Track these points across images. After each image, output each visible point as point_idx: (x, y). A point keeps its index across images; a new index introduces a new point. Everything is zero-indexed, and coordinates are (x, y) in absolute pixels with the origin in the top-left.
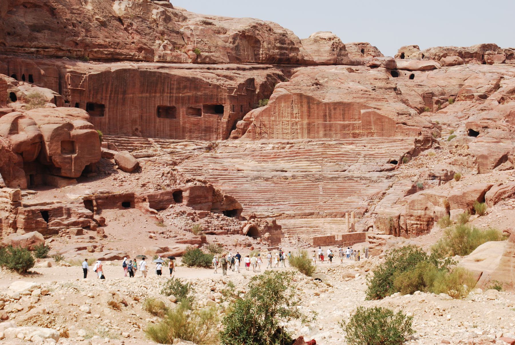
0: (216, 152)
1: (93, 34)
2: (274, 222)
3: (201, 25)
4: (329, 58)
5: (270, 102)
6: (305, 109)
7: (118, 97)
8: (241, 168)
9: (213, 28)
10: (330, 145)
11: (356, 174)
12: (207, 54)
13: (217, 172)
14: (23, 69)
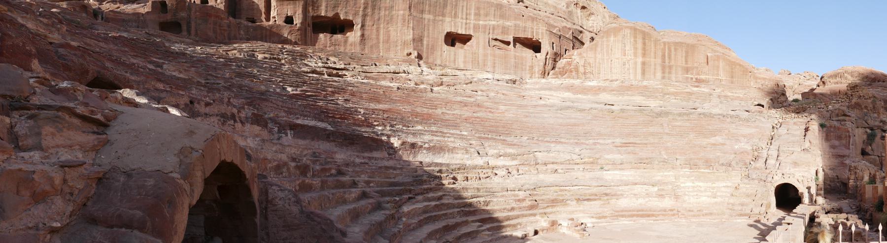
6: (640, 45)
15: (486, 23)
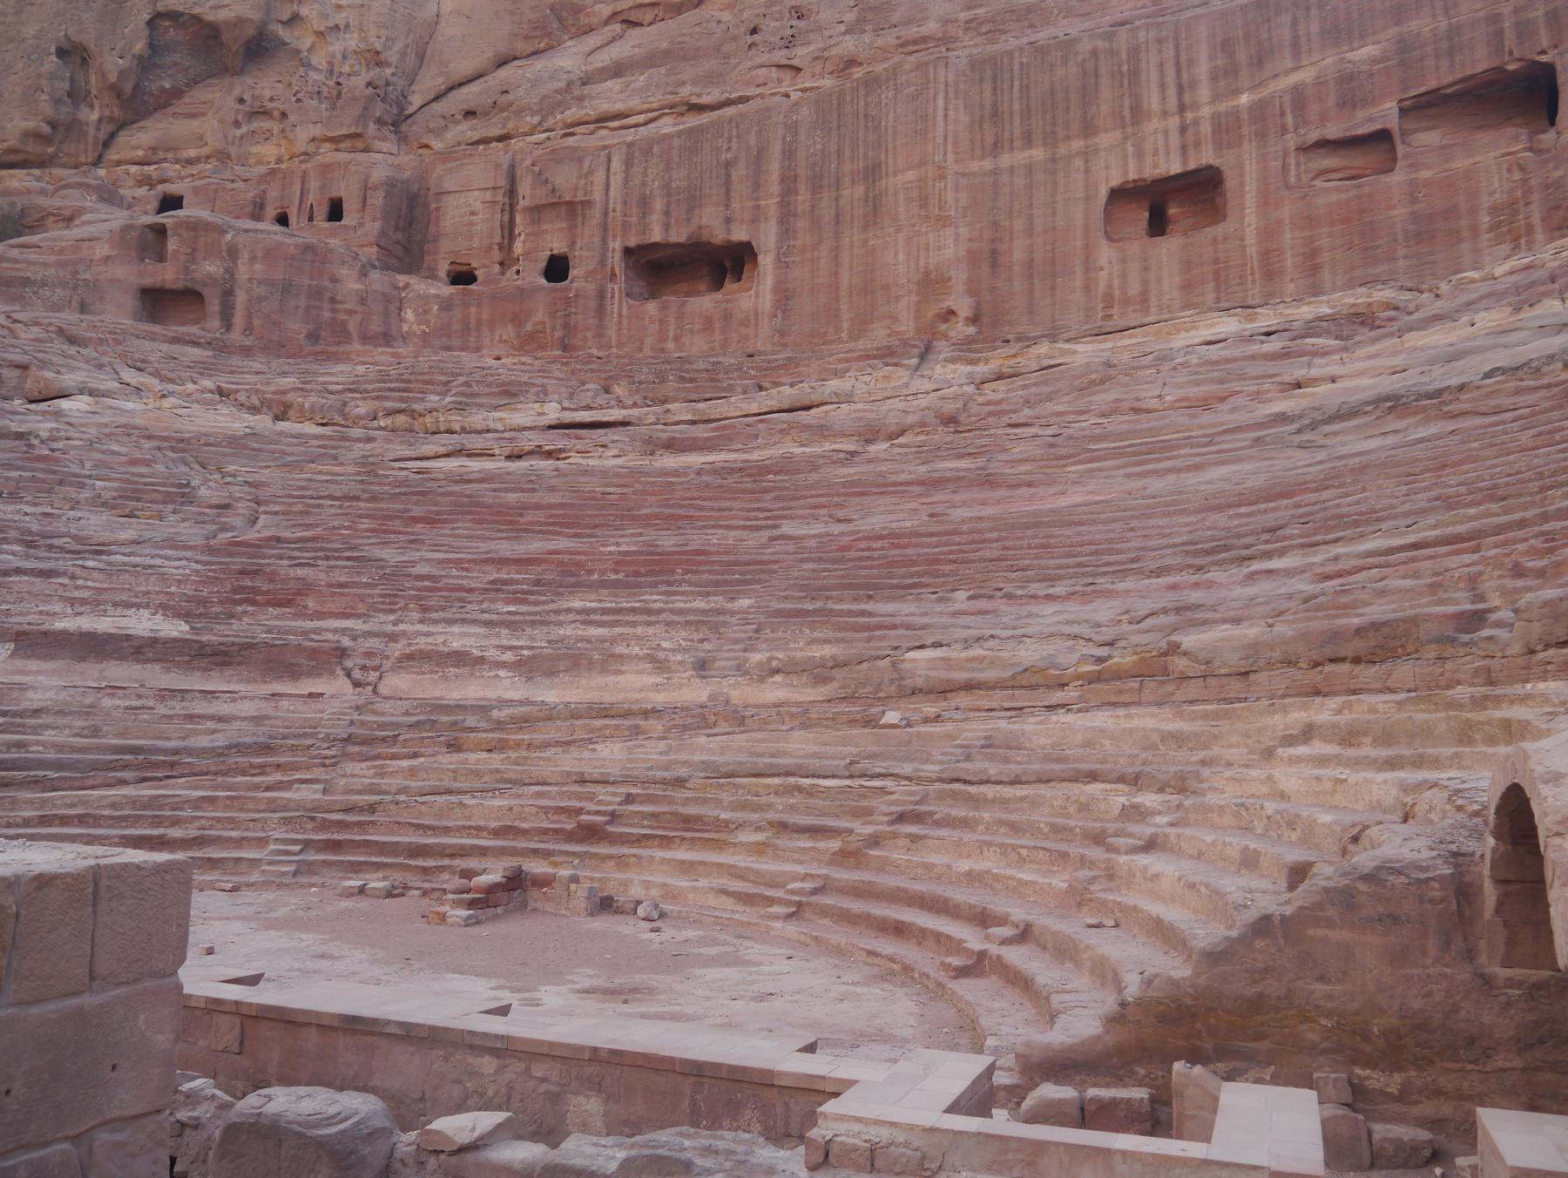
1: (896, 17)
7: (837, 199)
14: (313, 185)
15: (1265, 92)
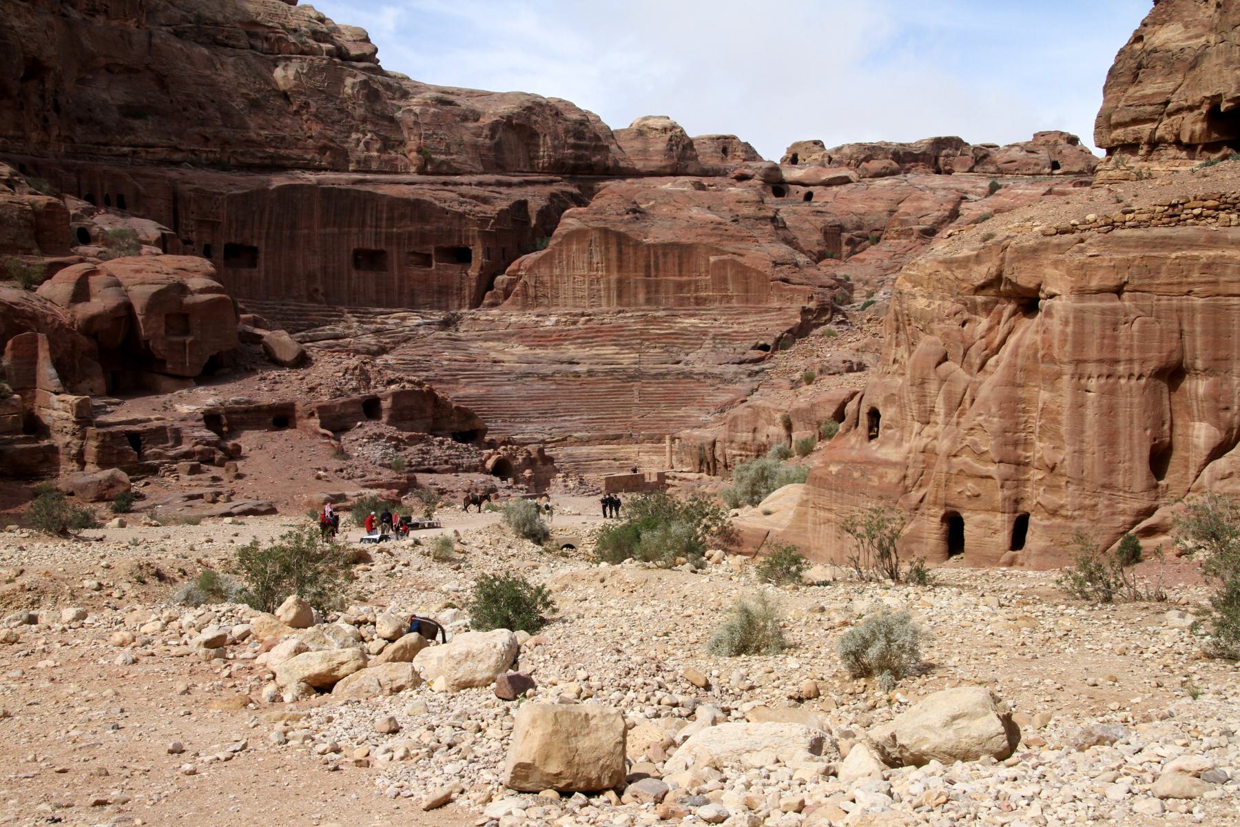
0: (457, 330)
2: (541, 451)
3: (434, 106)
4: (663, 164)
5: (552, 242)
6: (613, 255)
8: (500, 357)
9: (455, 110)
10: (655, 318)
11: (699, 367)
12: (443, 157)
13: (456, 365)
